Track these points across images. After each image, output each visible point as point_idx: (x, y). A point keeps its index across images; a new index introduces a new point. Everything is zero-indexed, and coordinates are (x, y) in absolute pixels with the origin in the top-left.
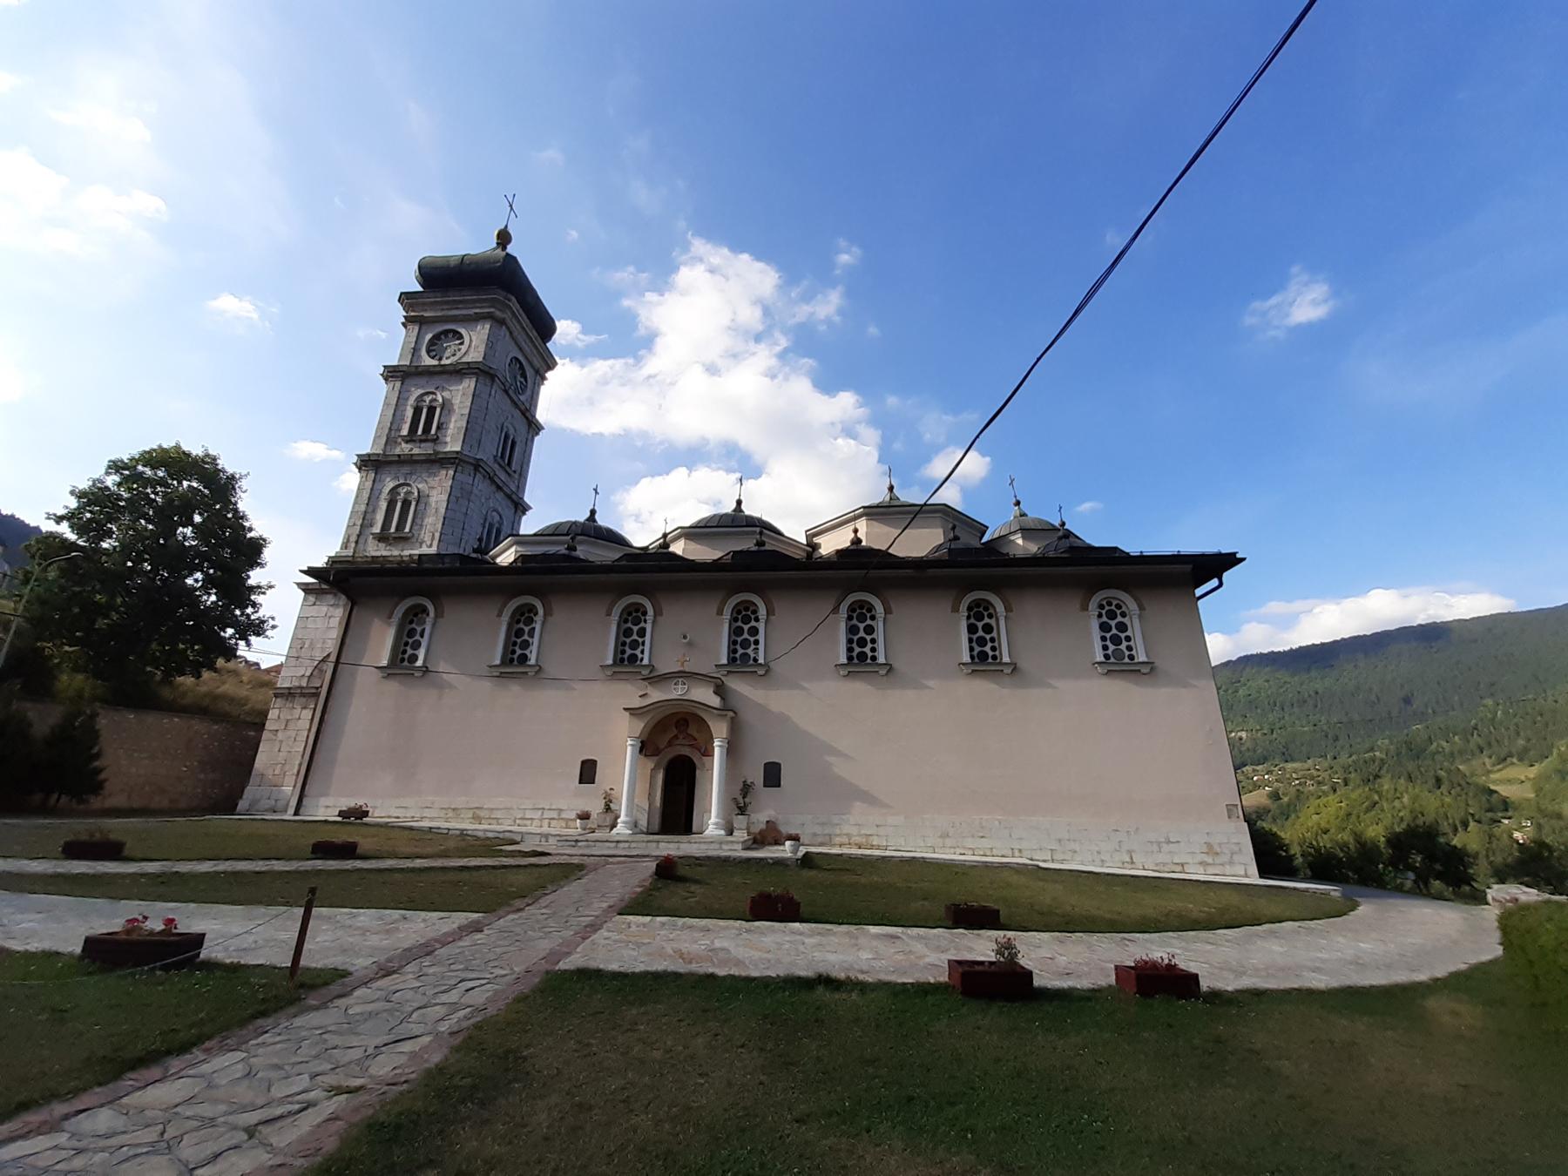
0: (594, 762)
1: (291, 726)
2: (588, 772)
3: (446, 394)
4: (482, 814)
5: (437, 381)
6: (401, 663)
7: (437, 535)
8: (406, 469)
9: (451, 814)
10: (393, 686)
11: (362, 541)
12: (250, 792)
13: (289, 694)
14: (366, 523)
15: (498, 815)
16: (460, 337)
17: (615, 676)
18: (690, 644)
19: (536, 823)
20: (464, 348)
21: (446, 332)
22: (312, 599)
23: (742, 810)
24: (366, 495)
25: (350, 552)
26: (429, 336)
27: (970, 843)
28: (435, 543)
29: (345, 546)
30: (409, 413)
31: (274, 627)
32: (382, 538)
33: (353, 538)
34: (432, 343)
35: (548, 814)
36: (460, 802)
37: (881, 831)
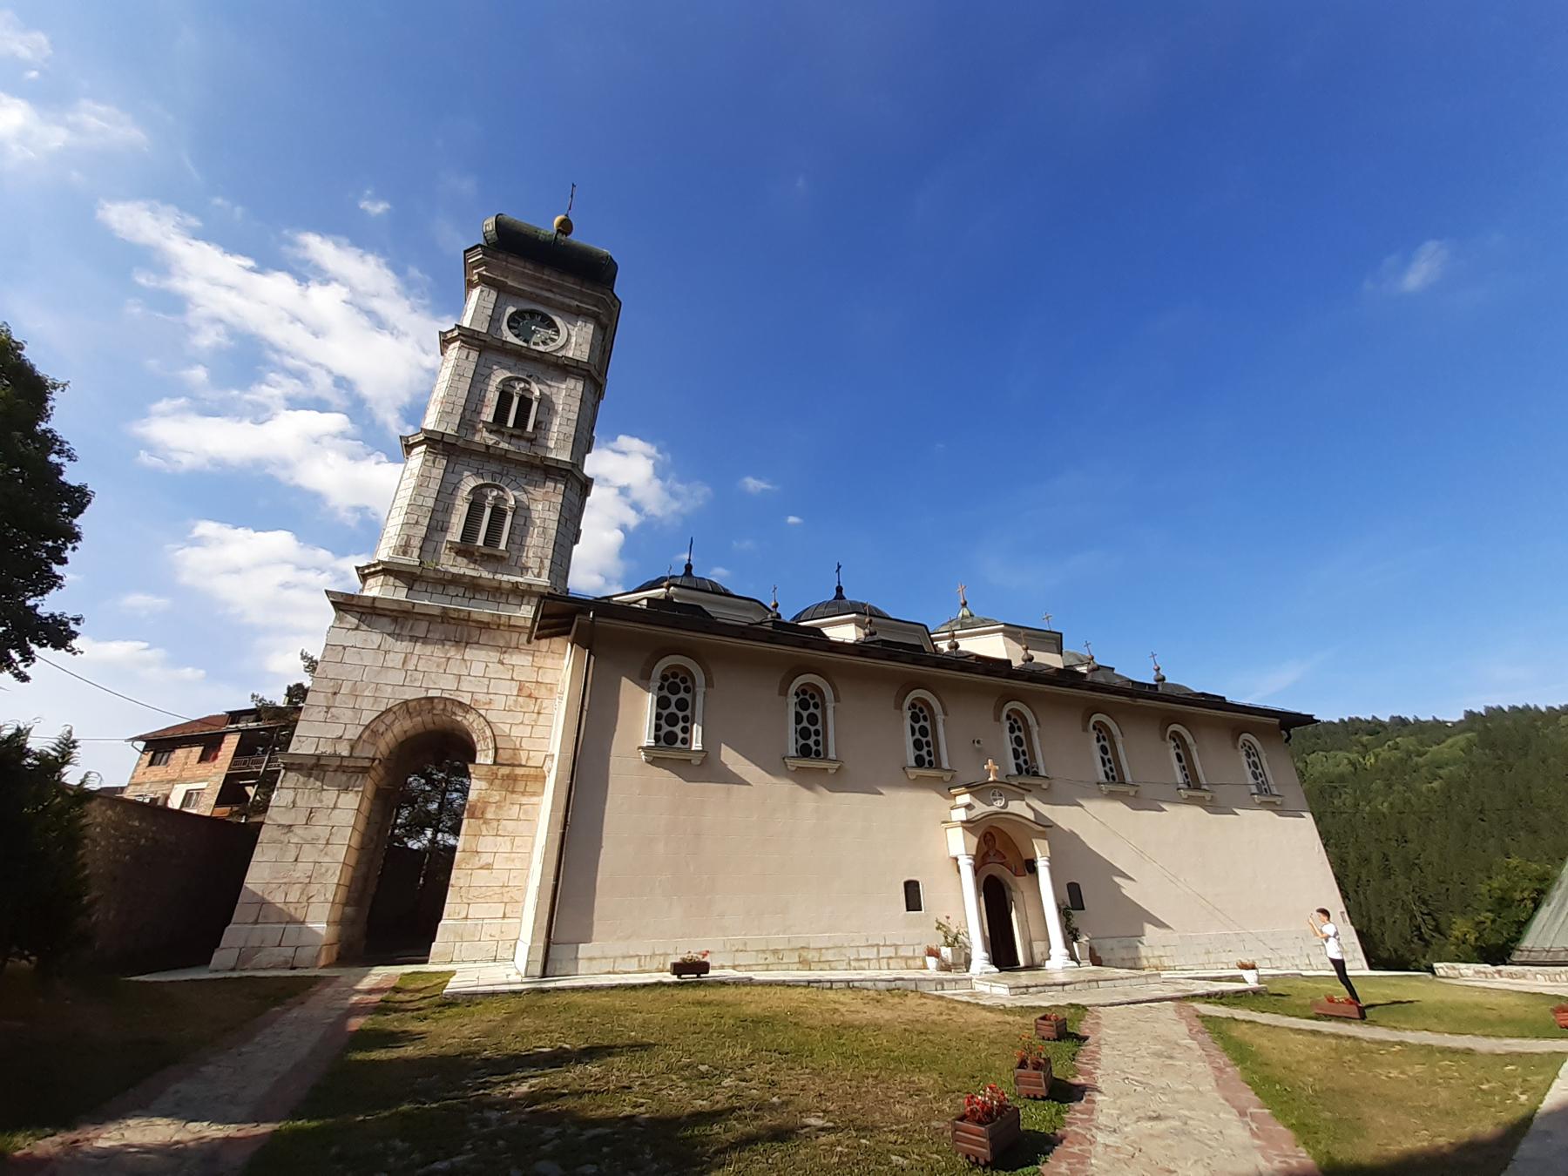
0: (916, 883)
1: (320, 818)
2: (912, 896)
3: (546, 390)
4: (810, 955)
5: (531, 368)
6: (667, 741)
7: (547, 563)
8: (494, 467)
9: (771, 959)
10: (664, 777)
11: (430, 547)
12: (235, 935)
13: (315, 767)
14: (437, 526)
15: (829, 955)
16: (552, 325)
17: (919, 783)
18: (979, 751)
19: (874, 964)
20: (561, 341)
21: (533, 313)
22: (352, 620)
23: (1075, 939)
24: (434, 486)
25: (413, 559)
26: (511, 310)
27: (1224, 957)
28: (545, 573)
29: (405, 549)
30: (492, 396)
31: (74, 635)
32: (464, 549)
33: (416, 542)
34: (512, 318)
35: (884, 952)
36: (779, 940)
37: (1168, 951)
